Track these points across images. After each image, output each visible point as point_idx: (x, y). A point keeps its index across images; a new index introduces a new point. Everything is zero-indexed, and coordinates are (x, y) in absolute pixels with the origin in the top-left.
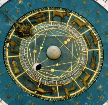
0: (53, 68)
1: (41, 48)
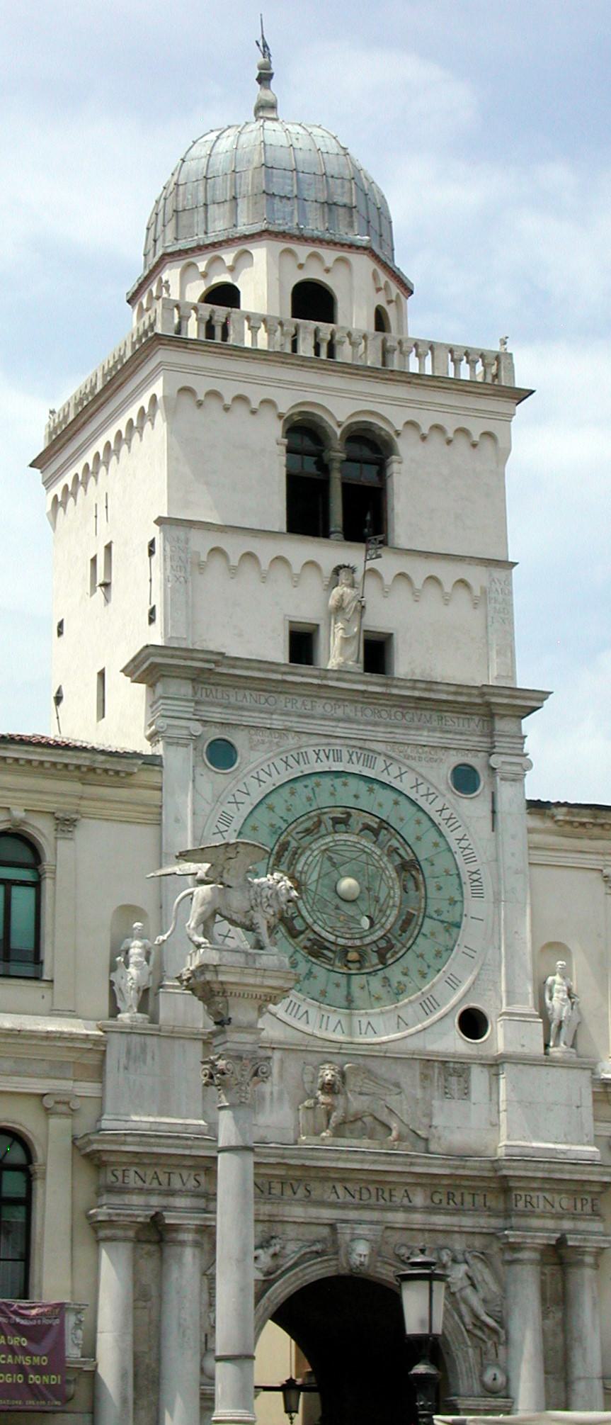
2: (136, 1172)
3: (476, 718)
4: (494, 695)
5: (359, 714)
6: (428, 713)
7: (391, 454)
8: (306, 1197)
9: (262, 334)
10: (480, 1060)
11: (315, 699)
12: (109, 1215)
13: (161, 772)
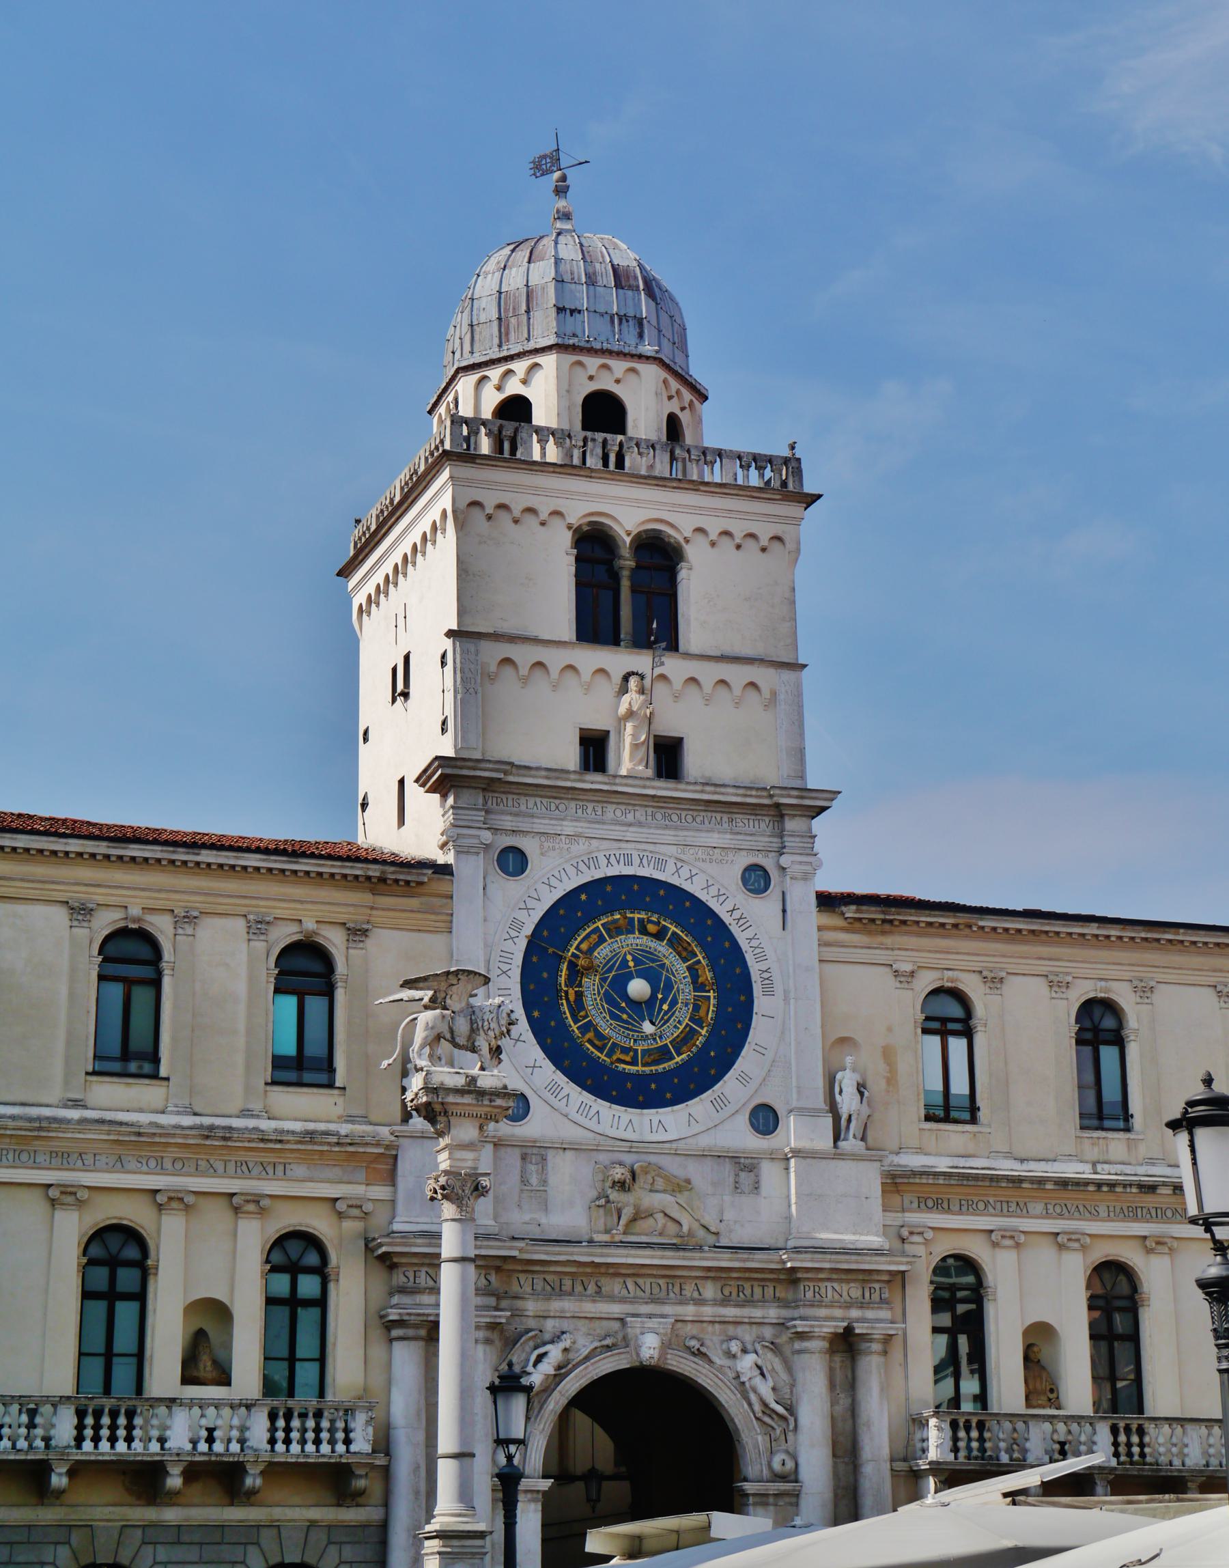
0: (661, 1005)
1: (623, 1005)
2: (427, 1272)
3: (767, 819)
4: (782, 796)
5: (650, 818)
6: (718, 816)
7: (683, 561)
8: (596, 1292)
9: (551, 446)
11: (605, 805)
12: (400, 1314)
13: (452, 881)
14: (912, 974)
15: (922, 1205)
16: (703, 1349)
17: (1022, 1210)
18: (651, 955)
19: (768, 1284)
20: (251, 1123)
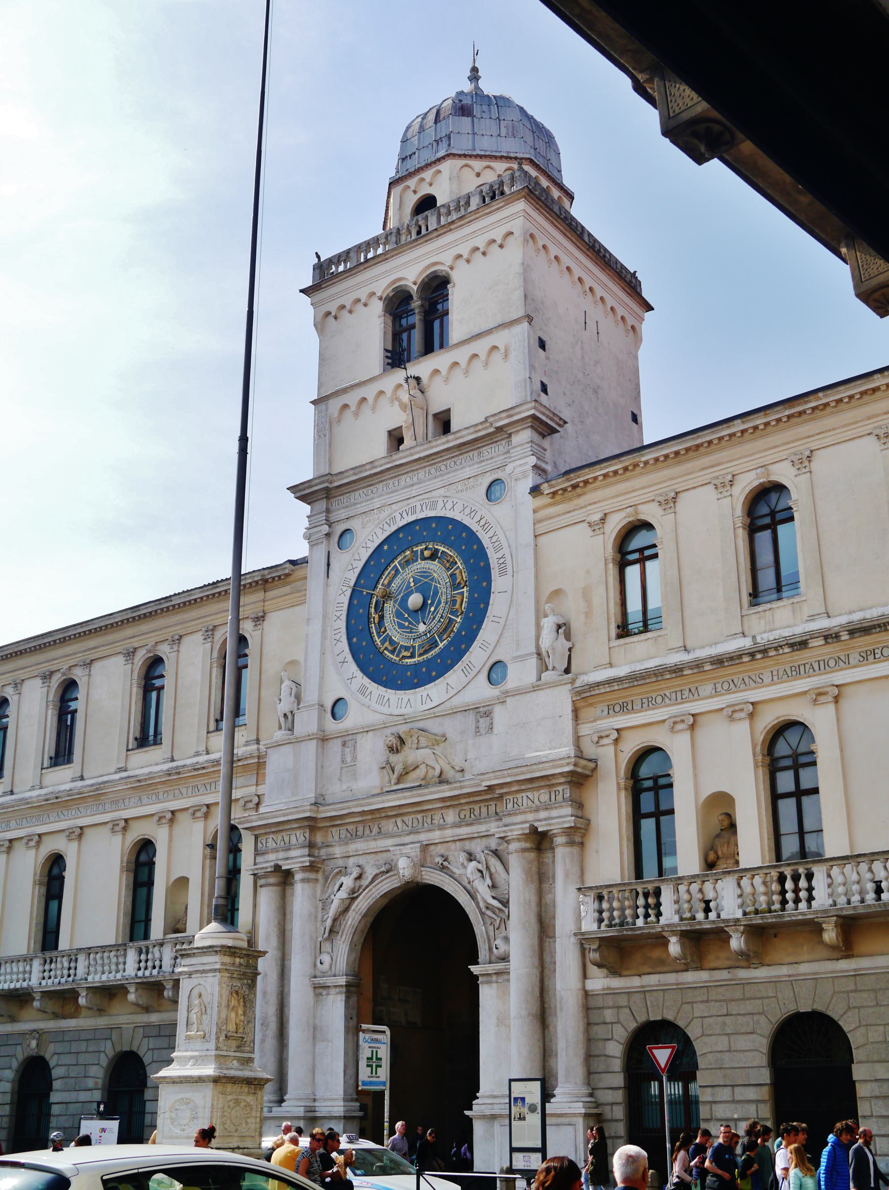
0: (430, 608)
3: (503, 442)
4: (496, 421)
6: (471, 454)
8: (378, 833)
10: (498, 699)
14: (603, 520)
15: (611, 712)
16: (445, 863)
17: (694, 694)
18: (425, 574)
19: (491, 803)
20: (195, 760)
